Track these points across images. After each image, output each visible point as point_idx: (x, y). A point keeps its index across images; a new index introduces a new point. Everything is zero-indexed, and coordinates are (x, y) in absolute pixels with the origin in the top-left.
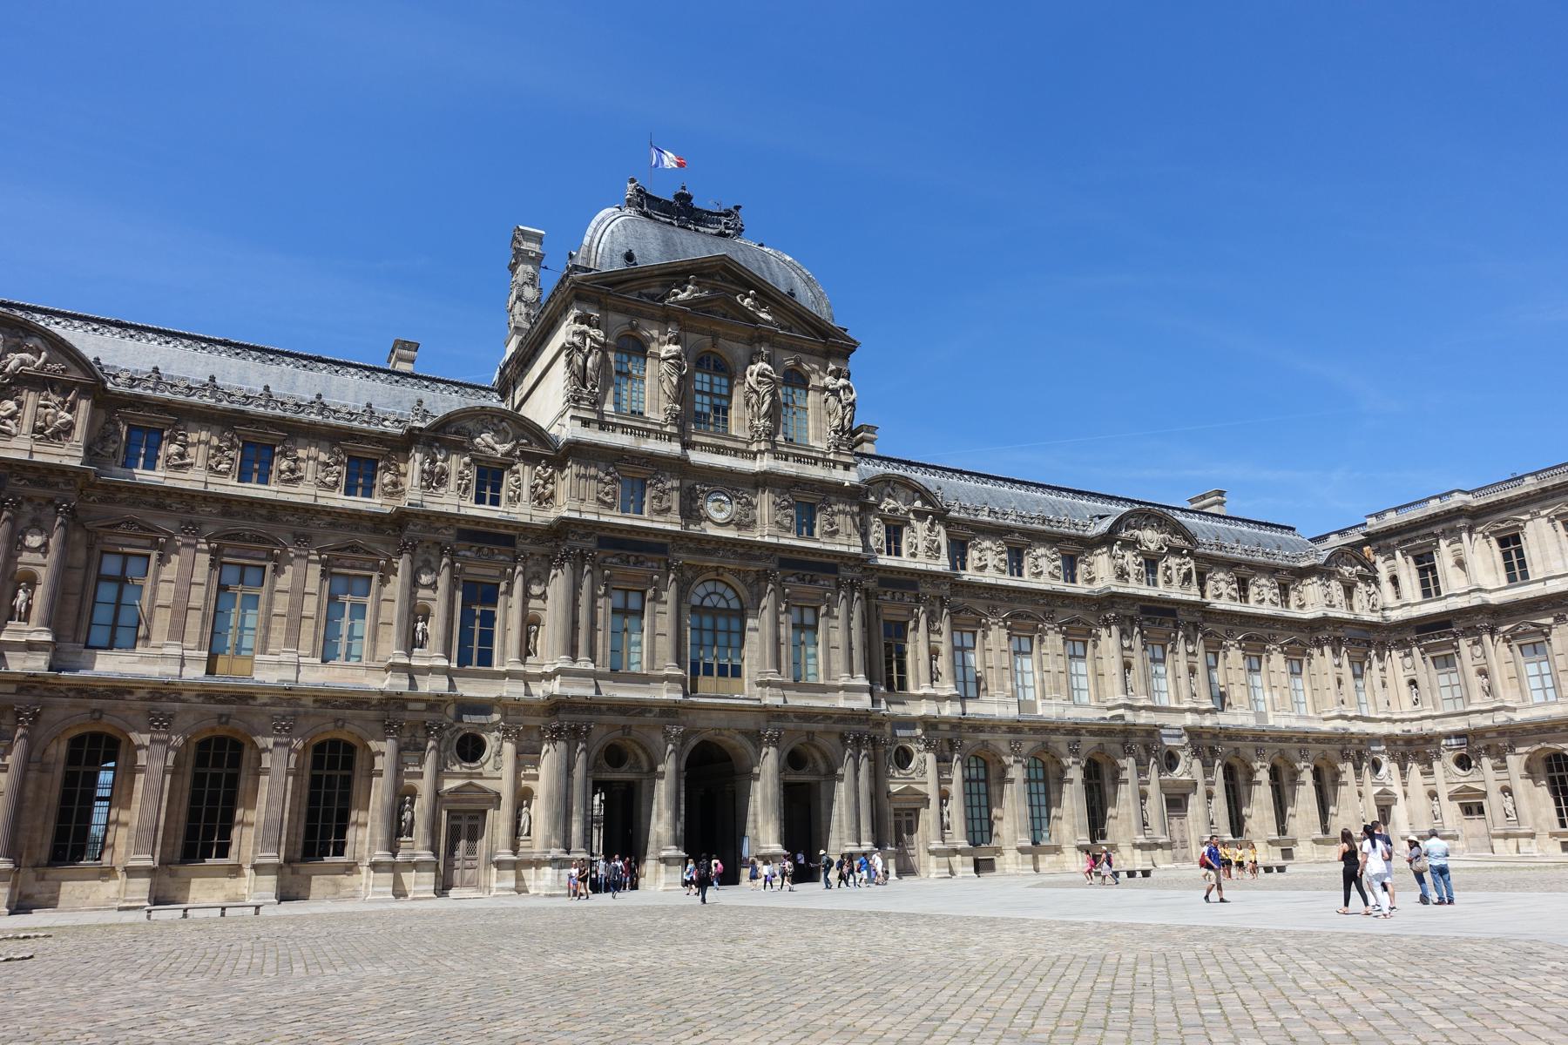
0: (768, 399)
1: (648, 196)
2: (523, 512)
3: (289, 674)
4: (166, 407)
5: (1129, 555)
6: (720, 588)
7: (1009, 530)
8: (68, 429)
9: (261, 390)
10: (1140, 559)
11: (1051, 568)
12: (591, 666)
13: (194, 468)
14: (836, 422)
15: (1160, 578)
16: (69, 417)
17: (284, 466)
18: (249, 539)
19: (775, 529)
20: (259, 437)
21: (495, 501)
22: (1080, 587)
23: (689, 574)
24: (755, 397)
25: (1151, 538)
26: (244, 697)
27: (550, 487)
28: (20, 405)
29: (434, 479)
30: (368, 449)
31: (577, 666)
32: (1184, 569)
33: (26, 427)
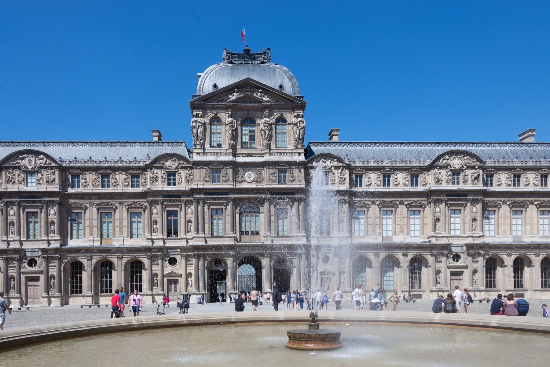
0: (267, 132)
1: (232, 54)
2: (182, 187)
3: (121, 243)
4: (79, 168)
5: (443, 172)
6: (251, 205)
7: (384, 168)
8: (54, 180)
9: (104, 159)
10: (450, 173)
11: (404, 181)
12: (203, 235)
13: (90, 184)
14: (296, 137)
15: (461, 181)
16: (54, 177)
17: (113, 182)
18: (106, 203)
19: (269, 183)
20: (105, 173)
21: (174, 184)
22: (420, 188)
23: (238, 201)
24: (263, 132)
25: (457, 162)
26: (108, 250)
27: (191, 177)
28: (42, 175)
29: (154, 179)
30: (136, 172)
31: (199, 235)
32: (475, 175)
33: (45, 182)
